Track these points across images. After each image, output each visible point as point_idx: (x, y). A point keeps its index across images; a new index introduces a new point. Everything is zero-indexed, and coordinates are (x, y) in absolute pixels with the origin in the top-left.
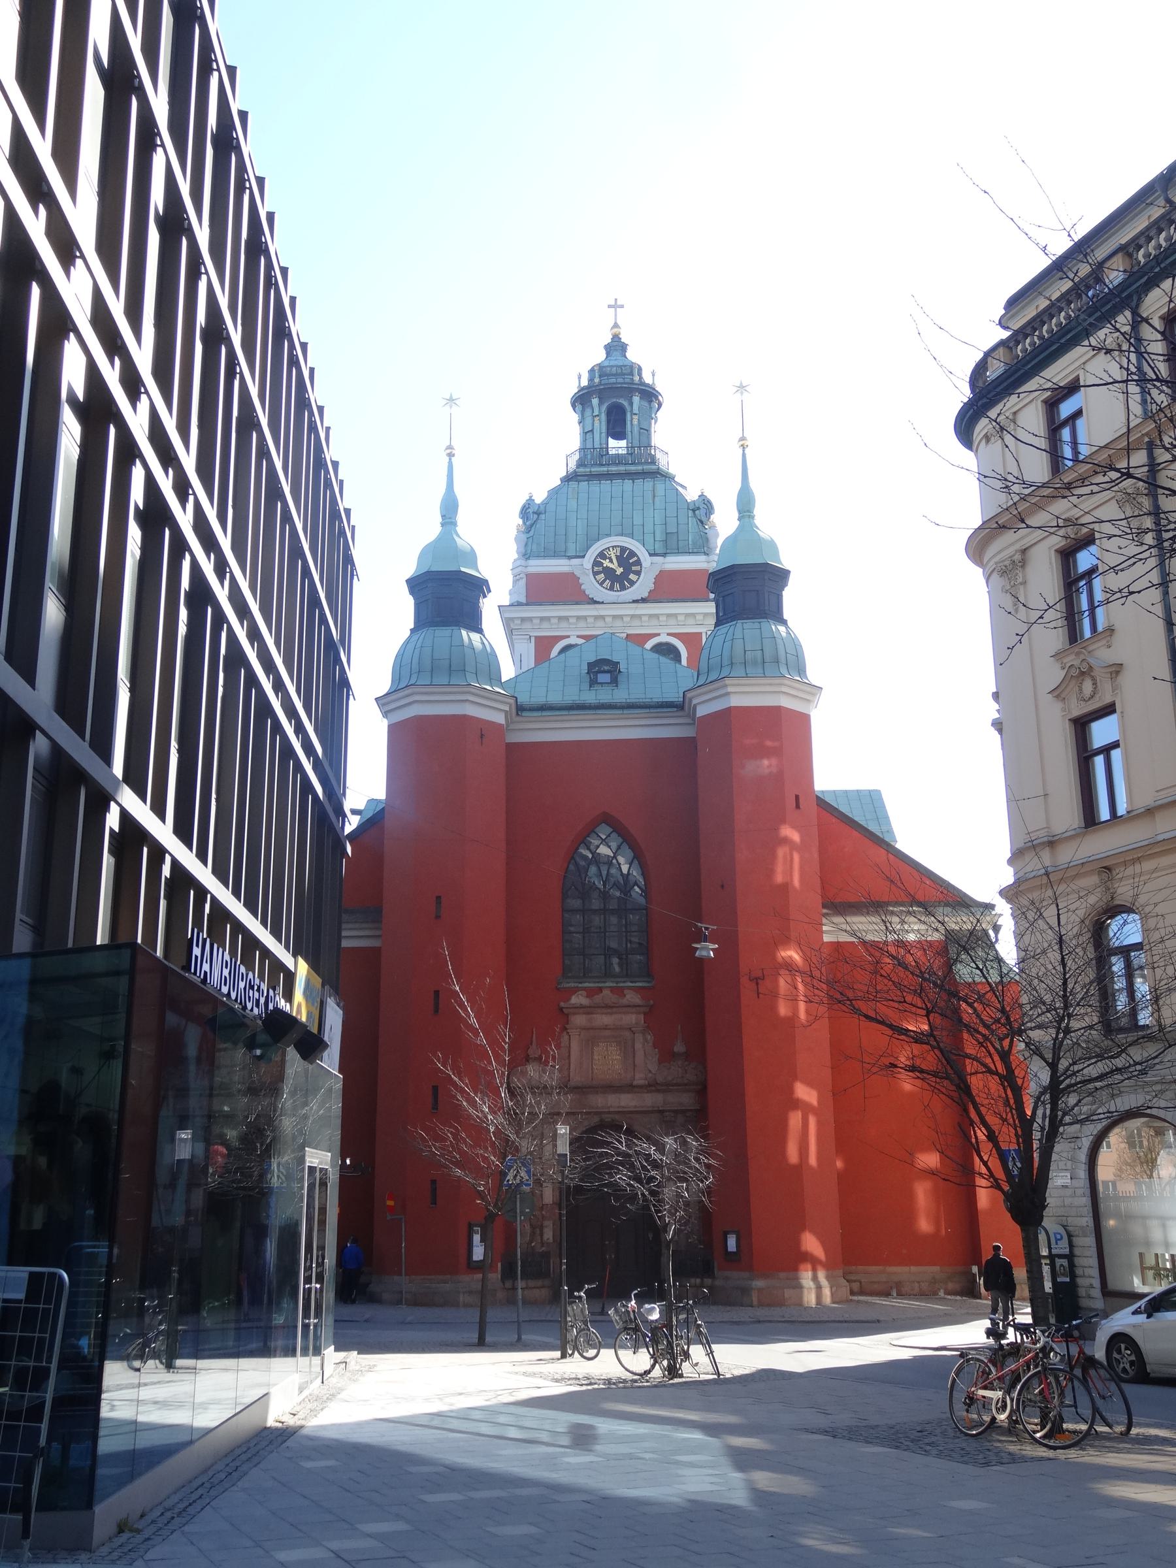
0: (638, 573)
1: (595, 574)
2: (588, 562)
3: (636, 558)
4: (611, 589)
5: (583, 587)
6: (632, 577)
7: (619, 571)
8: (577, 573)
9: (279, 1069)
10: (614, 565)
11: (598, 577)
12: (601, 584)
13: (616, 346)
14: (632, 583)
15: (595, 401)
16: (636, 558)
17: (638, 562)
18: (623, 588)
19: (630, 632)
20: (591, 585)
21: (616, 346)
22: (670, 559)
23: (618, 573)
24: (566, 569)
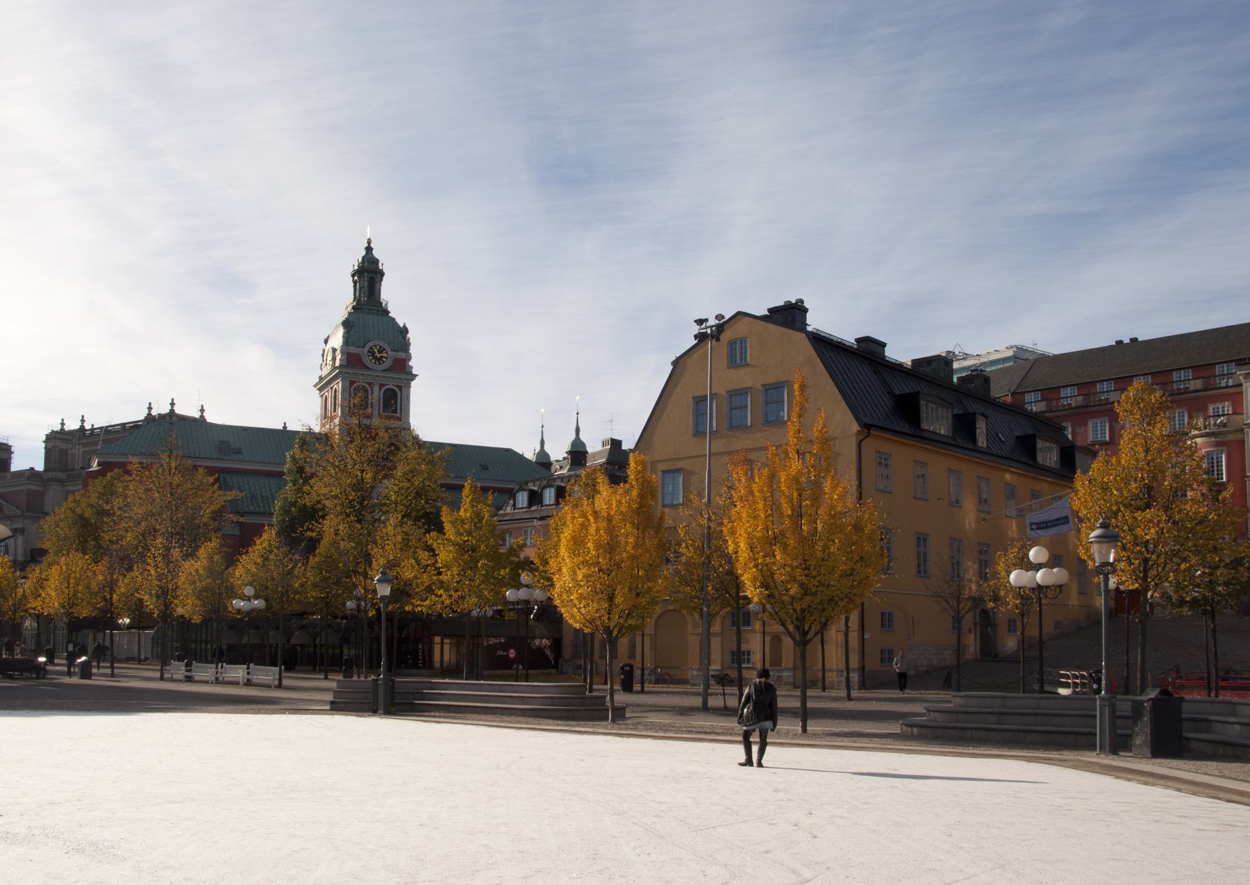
2: (366, 350)
4: (375, 363)
8: (361, 353)
13: (369, 249)
14: (384, 362)
15: (366, 274)
18: (380, 363)
20: (367, 360)
21: (369, 249)
24: (356, 352)
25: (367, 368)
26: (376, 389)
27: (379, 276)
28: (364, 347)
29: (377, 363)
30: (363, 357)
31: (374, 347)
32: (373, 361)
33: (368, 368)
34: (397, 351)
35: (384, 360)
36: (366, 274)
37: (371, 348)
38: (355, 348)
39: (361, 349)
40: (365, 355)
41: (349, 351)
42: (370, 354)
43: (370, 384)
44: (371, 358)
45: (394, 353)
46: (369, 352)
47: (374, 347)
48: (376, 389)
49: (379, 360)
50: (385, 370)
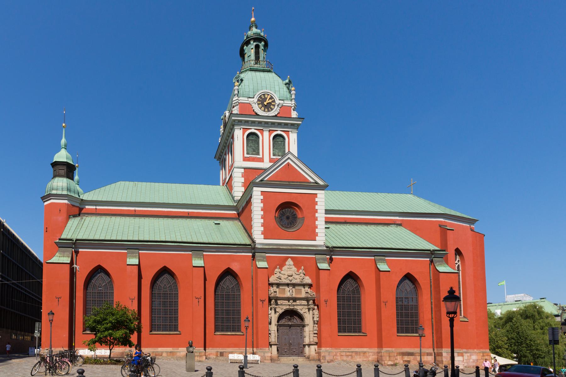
0: (274, 105)
1: (258, 104)
2: (255, 100)
3: (273, 99)
4: (264, 111)
5: (253, 108)
6: (272, 106)
7: (265, 103)
9: (216, 293)
11: (259, 106)
12: (260, 108)
14: (272, 109)
16: (273, 99)
18: (269, 111)
19: (270, 129)
20: (257, 109)
22: (285, 102)
24: (248, 102)
26: (266, 134)
27: (263, 43)
29: (266, 110)
30: (253, 105)
32: (263, 108)
33: (258, 115)
35: (272, 106)
36: (252, 42)
37: (260, 97)
38: (247, 99)
42: (260, 102)
43: (262, 131)
44: (260, 105)
46: (258, 100)
48: (266, 134)
49: (268, 107)
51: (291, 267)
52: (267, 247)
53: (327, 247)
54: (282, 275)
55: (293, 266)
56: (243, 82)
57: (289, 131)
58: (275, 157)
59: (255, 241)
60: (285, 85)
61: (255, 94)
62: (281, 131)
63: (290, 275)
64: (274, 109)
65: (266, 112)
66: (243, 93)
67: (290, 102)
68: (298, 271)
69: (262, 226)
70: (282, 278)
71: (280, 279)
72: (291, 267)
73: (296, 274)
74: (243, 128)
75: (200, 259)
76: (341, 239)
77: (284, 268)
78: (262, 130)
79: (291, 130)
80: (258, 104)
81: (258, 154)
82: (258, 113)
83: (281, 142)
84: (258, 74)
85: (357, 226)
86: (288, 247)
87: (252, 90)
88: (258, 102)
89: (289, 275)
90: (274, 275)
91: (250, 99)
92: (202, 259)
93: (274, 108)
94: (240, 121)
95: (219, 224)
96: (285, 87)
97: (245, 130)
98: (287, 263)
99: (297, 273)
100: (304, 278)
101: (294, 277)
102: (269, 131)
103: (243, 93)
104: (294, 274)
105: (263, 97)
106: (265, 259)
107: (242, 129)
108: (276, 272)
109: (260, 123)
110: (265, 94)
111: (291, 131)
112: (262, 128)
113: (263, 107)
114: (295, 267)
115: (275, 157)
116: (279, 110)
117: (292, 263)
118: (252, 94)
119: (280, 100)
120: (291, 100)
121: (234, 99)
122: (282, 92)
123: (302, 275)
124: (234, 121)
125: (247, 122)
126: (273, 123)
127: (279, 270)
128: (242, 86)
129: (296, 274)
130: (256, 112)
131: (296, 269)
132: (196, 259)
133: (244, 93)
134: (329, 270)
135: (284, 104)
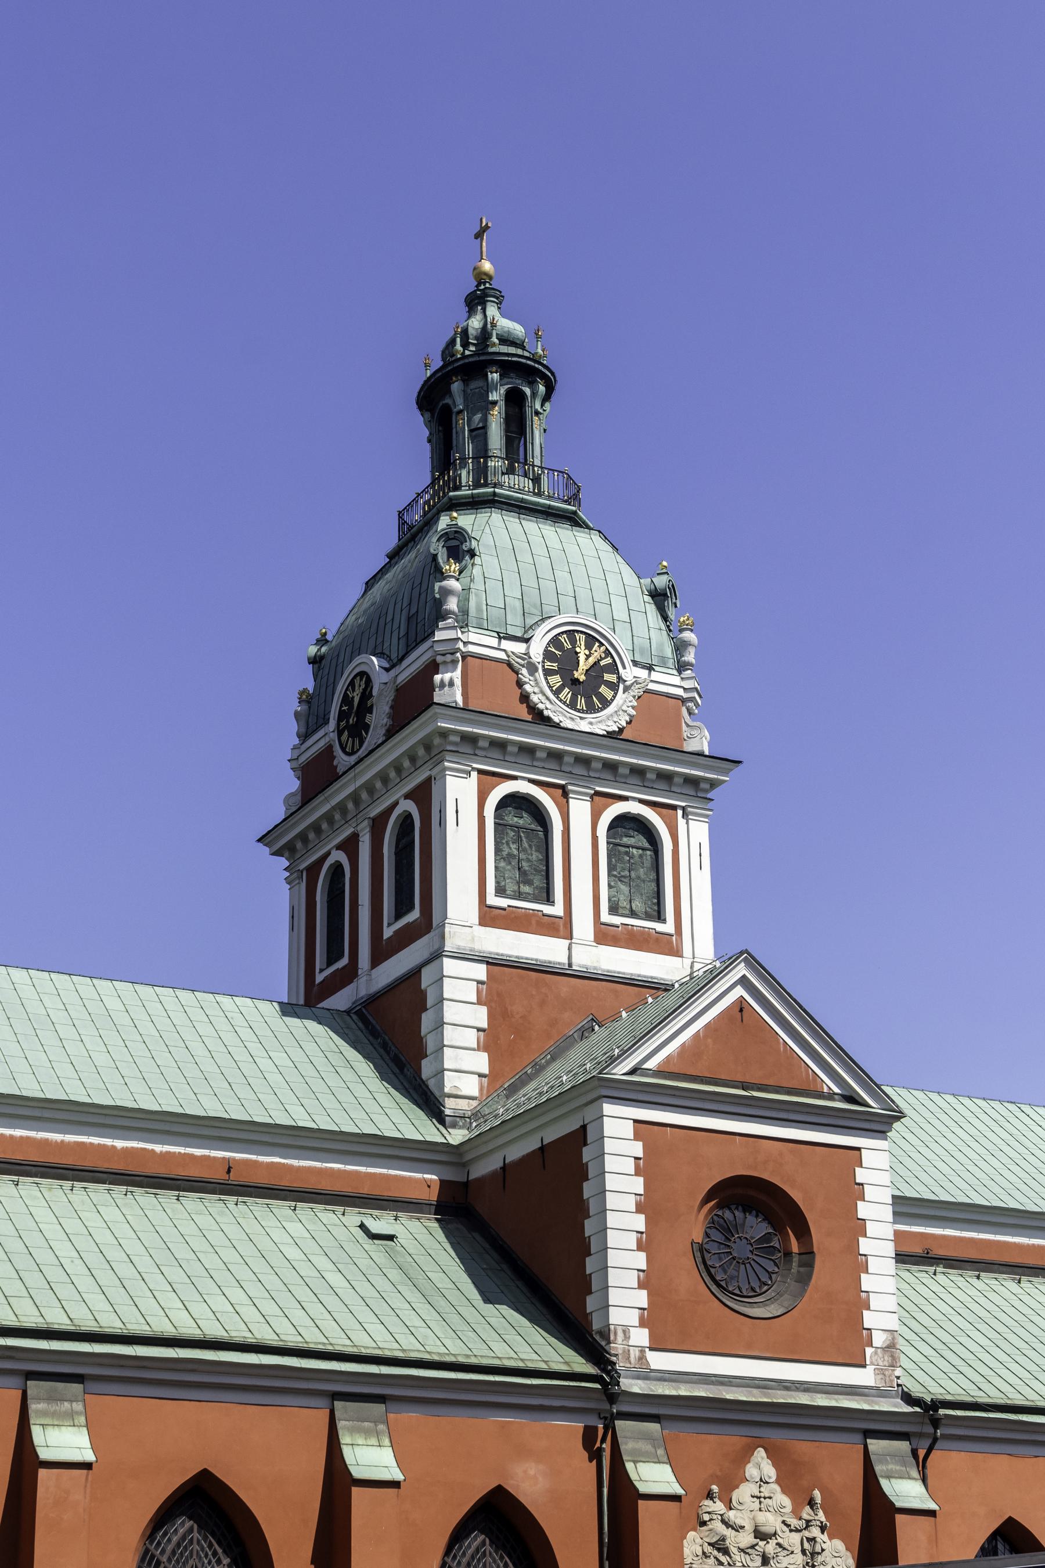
1: (548, 673)
2: (537, 649)
3: (609, 660)
4: (573, 705)
6: (603, 689)
8: (516, 661)
10: (583, 665)
12: (557, 693)
14: (606, 703)
17: (613, 668)
18: (591, 709)
19: (598, 789)
23: (576, 675)
24: (502, 655)
25: (540, 717)
26: (580, 809)
28: (527, 641)
29: (581, 703)
31: (581, 639)
34: (650, 668)
35: (603, 689)
37: (555, 641)
38: (494, 642)
39: (519, 648)
40: (532, 669)
41: (472, 648)
42: (555, 666)
44: (556, 680)
45: (643, 674)
46: (548, 655)
47: (581, 639)
48: (580, 809)
50: (610, 735)
51: (766, 1490)
52: (667, 1392)
53: (908, 1398)
54: (729, 1533)
55: (777, 1488)
56: (477, 560)
57: (674, 808)
58: (617, 920)
59: (614, 1359)
60: (648, 599)
61: (530, 621)
62: (641, 801)
63: (770, 1530)
64: (612, 700)
65: (579, 711)
66: (479, 610)
67: (676, 680)
68: (796, 1513)
69: (641, 1286)
70: (733, 1550)
71: (726, 1551)
72: (766, 1490)
73: (788, 1526)
74: (480, 772)
75: (373, 1441)
76: (943, 1353)
77: (735, 1495)
78: (563, 787)
79: (683, 804)
80: (544, 670)
81: (549, 900)
82: (546, 713)
83: (640, 851)
84: (532, 526)
85: (978, 1277)
86: (755, 1391)
87: (518, 604)
88: (548, 665)
89: (763, 1529)
90: (695, 1530)
91: (507, 645)
92: (387, 1442)
93: (614, 697)
94: (471, 740)
95: (391, 1238)
96: (653, 606)
97: (488, 779)
98: (751, 1471)
99: (794, 1522)
100: (823, 1550)
101: (780, 1540)
102: (592, 797)
103: (479, 610)
104: (779, 1527)
105: (563, 638)
106: (661, 1452)
107: (474, 774)
108: (706, 1517)
109: (556, 756)
110: (574, 631)
111: (684, 809)
112: (563, 782)
113: (567, 690)
114: (784, 1491)
115: (617, 920)
116: (633, 707)
117: (769, 1471)
118: (519, 621)
119: (635, 663)
120: (681, 667)
121: (439, 635)
122: (641, 631)
123: (815, 1532)
124: (444, 734)
125: (501, 745)
126: (611, 767)
127: (719, 1506)
128: (472, 580)
129: (788, 1526)
130: (540, 706)
131: (786, 1501)
132: (360, 1441)
133: (482, 611)
134: (932, 1513)
135: (652, 686)
